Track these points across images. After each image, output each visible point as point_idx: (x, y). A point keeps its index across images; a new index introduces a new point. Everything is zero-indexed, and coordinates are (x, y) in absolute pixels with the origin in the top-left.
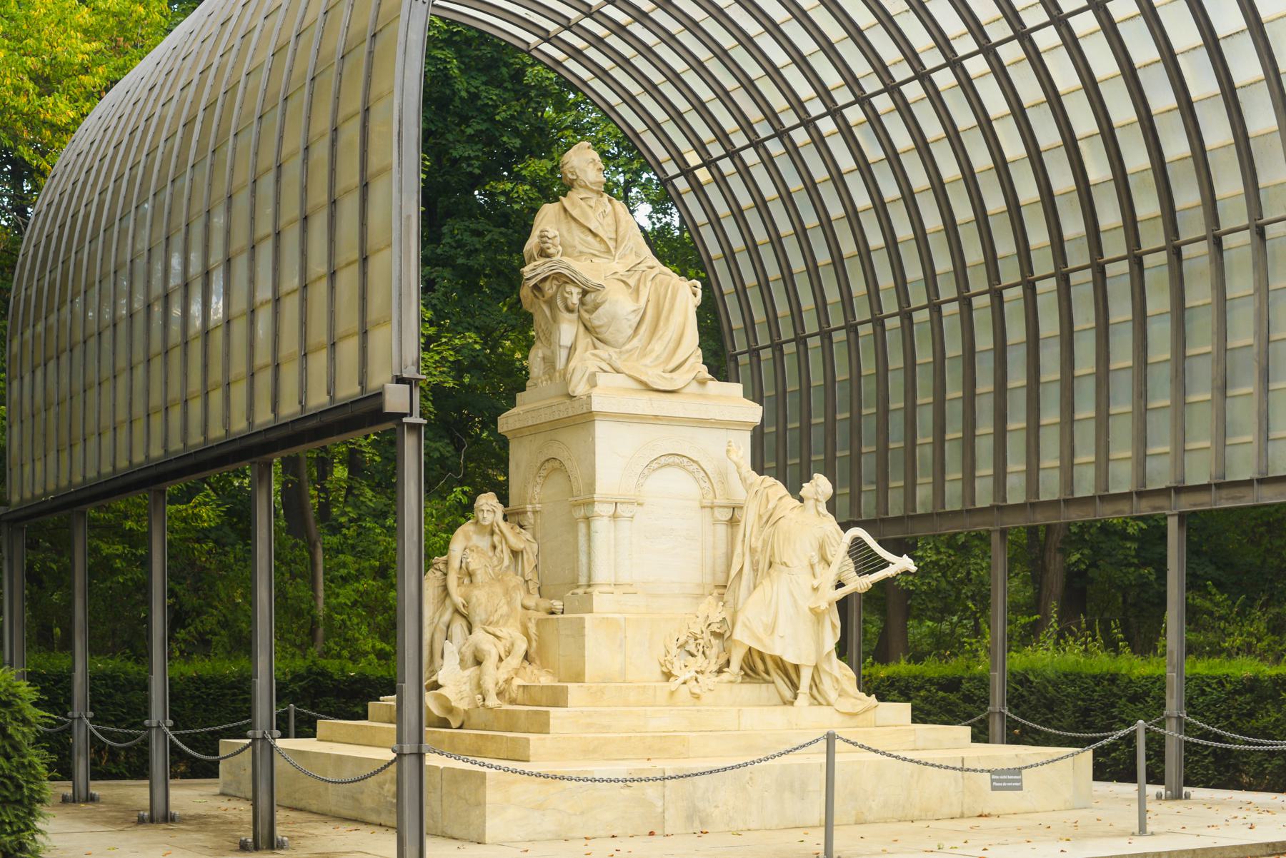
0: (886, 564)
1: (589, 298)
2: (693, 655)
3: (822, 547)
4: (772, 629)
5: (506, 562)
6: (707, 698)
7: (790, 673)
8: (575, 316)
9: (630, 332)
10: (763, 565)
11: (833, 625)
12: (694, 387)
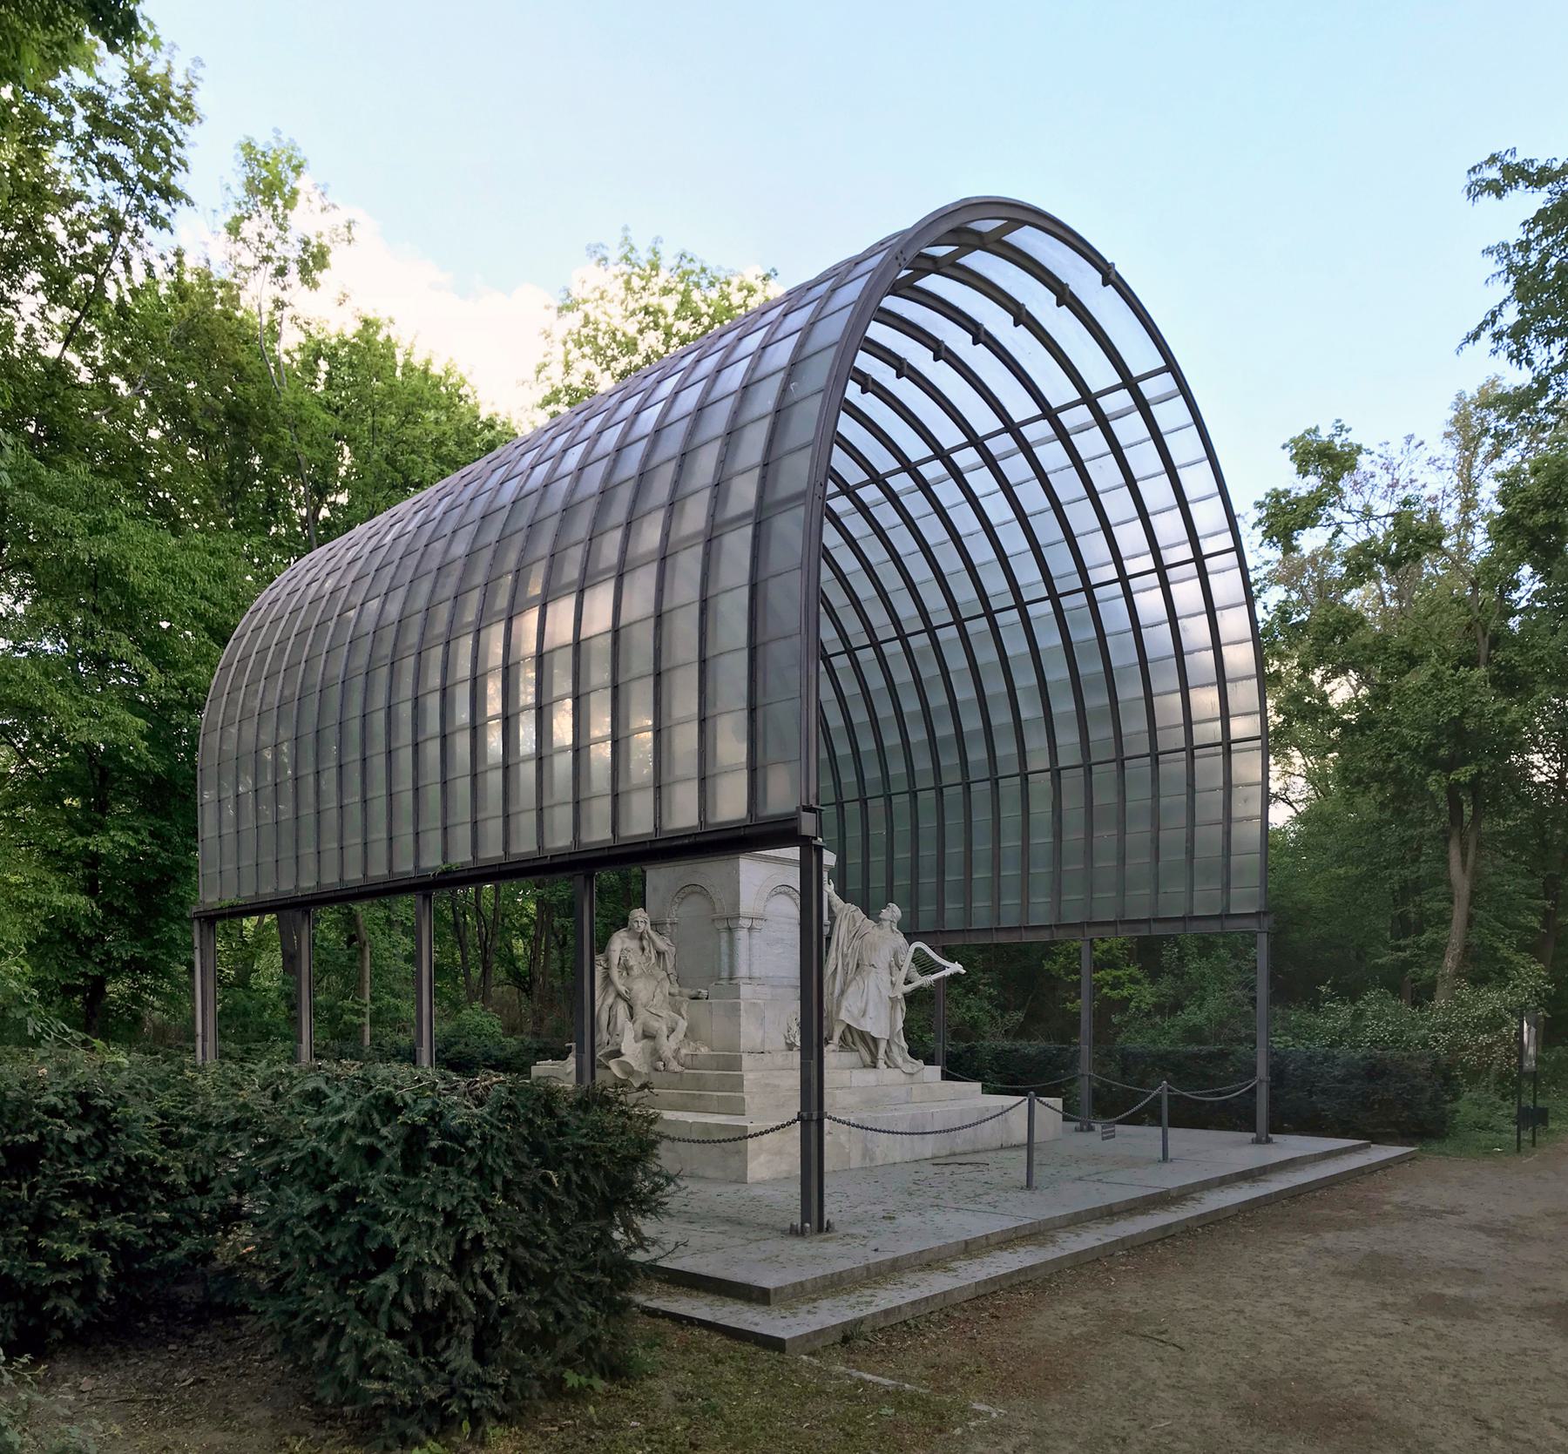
0: (944, 968)
3: (895, 955)
7: (870, 1042)
10: (852, 966)
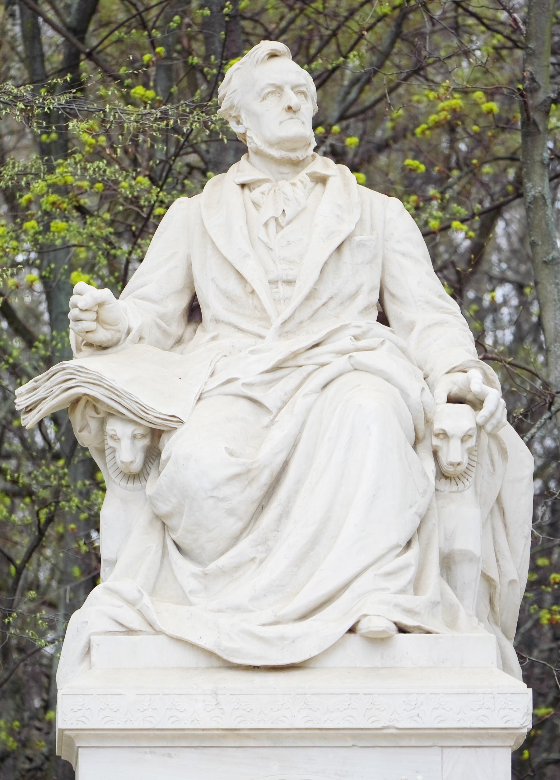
9: (233, 525)
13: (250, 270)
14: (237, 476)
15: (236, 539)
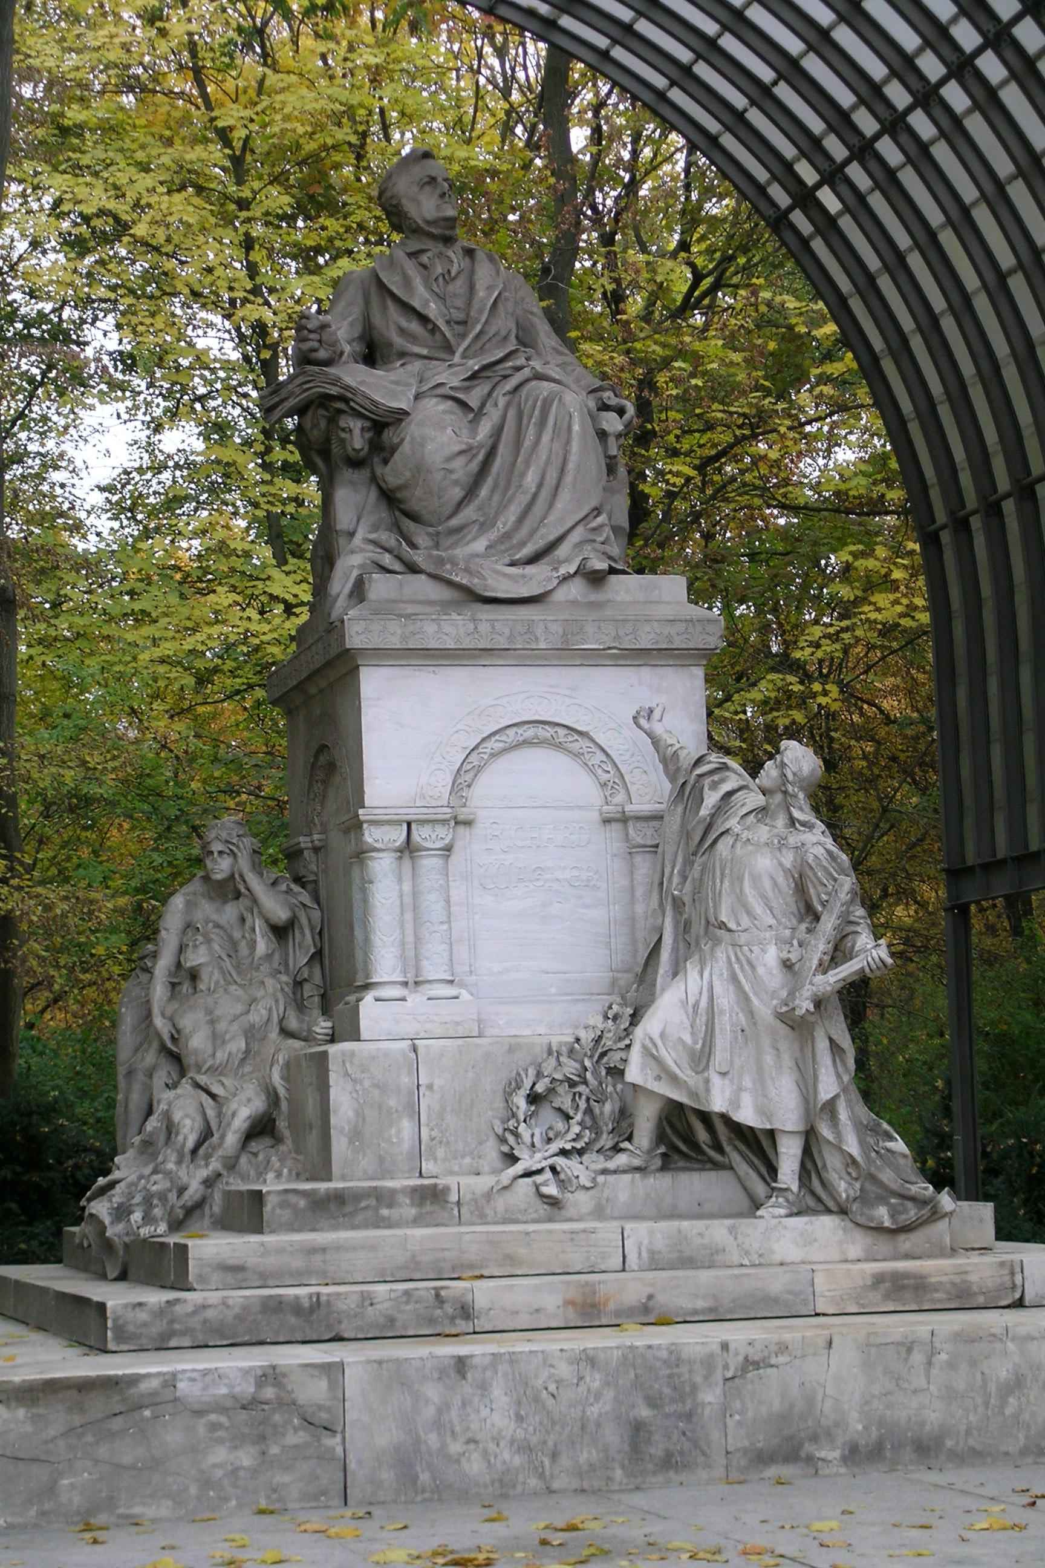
1: (389, 436)
2: (568, 1117)
3: (801, 889)
4: (701, 1059)
5: (262, 947)
6: (580, 1201)
8: (365, 473)
9: (457, 493)
11: (835, 1047)
12: (576, 589)
13: (433, 310)
14: (462, 452)
15: (459, 505)
